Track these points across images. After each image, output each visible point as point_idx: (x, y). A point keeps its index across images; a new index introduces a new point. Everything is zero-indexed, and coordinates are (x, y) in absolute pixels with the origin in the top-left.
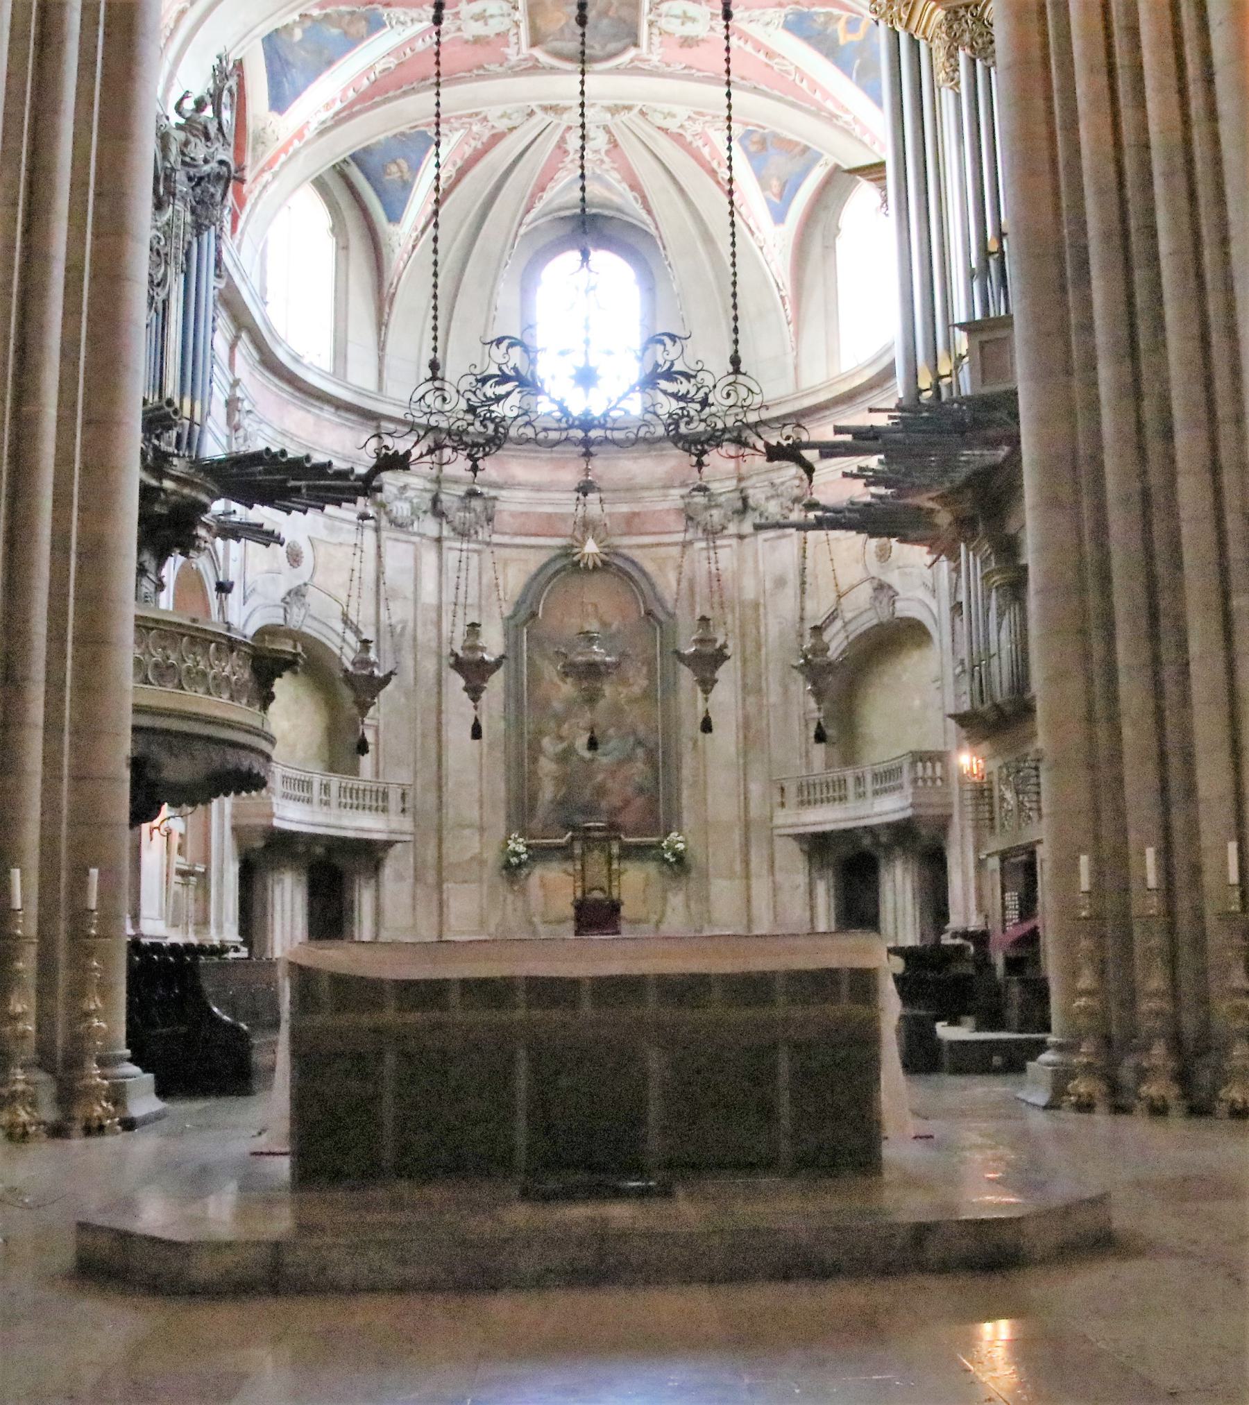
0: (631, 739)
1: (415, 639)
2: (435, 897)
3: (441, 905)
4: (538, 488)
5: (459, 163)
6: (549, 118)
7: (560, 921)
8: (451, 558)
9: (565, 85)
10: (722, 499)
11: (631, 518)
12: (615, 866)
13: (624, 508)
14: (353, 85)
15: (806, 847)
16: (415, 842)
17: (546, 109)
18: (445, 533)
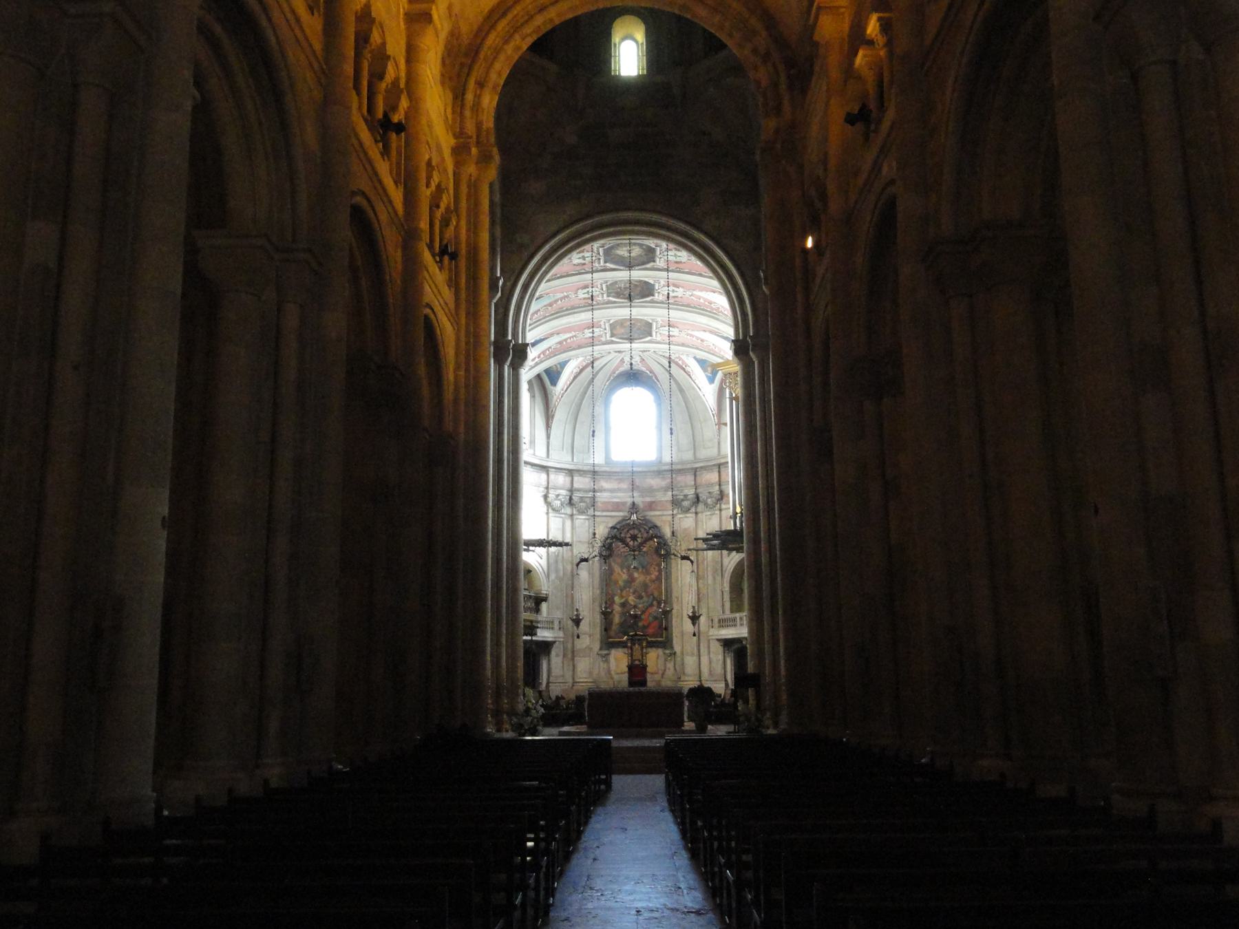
0: (652, 597)
1: (563, 557)
2: (571, 663)
3: (574, 666)
4: (612, 491)
5: (581, 367)
6: (616, 354)
7: (622, 673)
8: (577, 522)
9: (627, 346)
10: (689, 497)
11: (652, 503)
12: (644, 651)
13: (648, 499)
14: (543, 353)
15: (722, 644)
16: (563, 641)
17: (616, 352)
18: (574, 512)
